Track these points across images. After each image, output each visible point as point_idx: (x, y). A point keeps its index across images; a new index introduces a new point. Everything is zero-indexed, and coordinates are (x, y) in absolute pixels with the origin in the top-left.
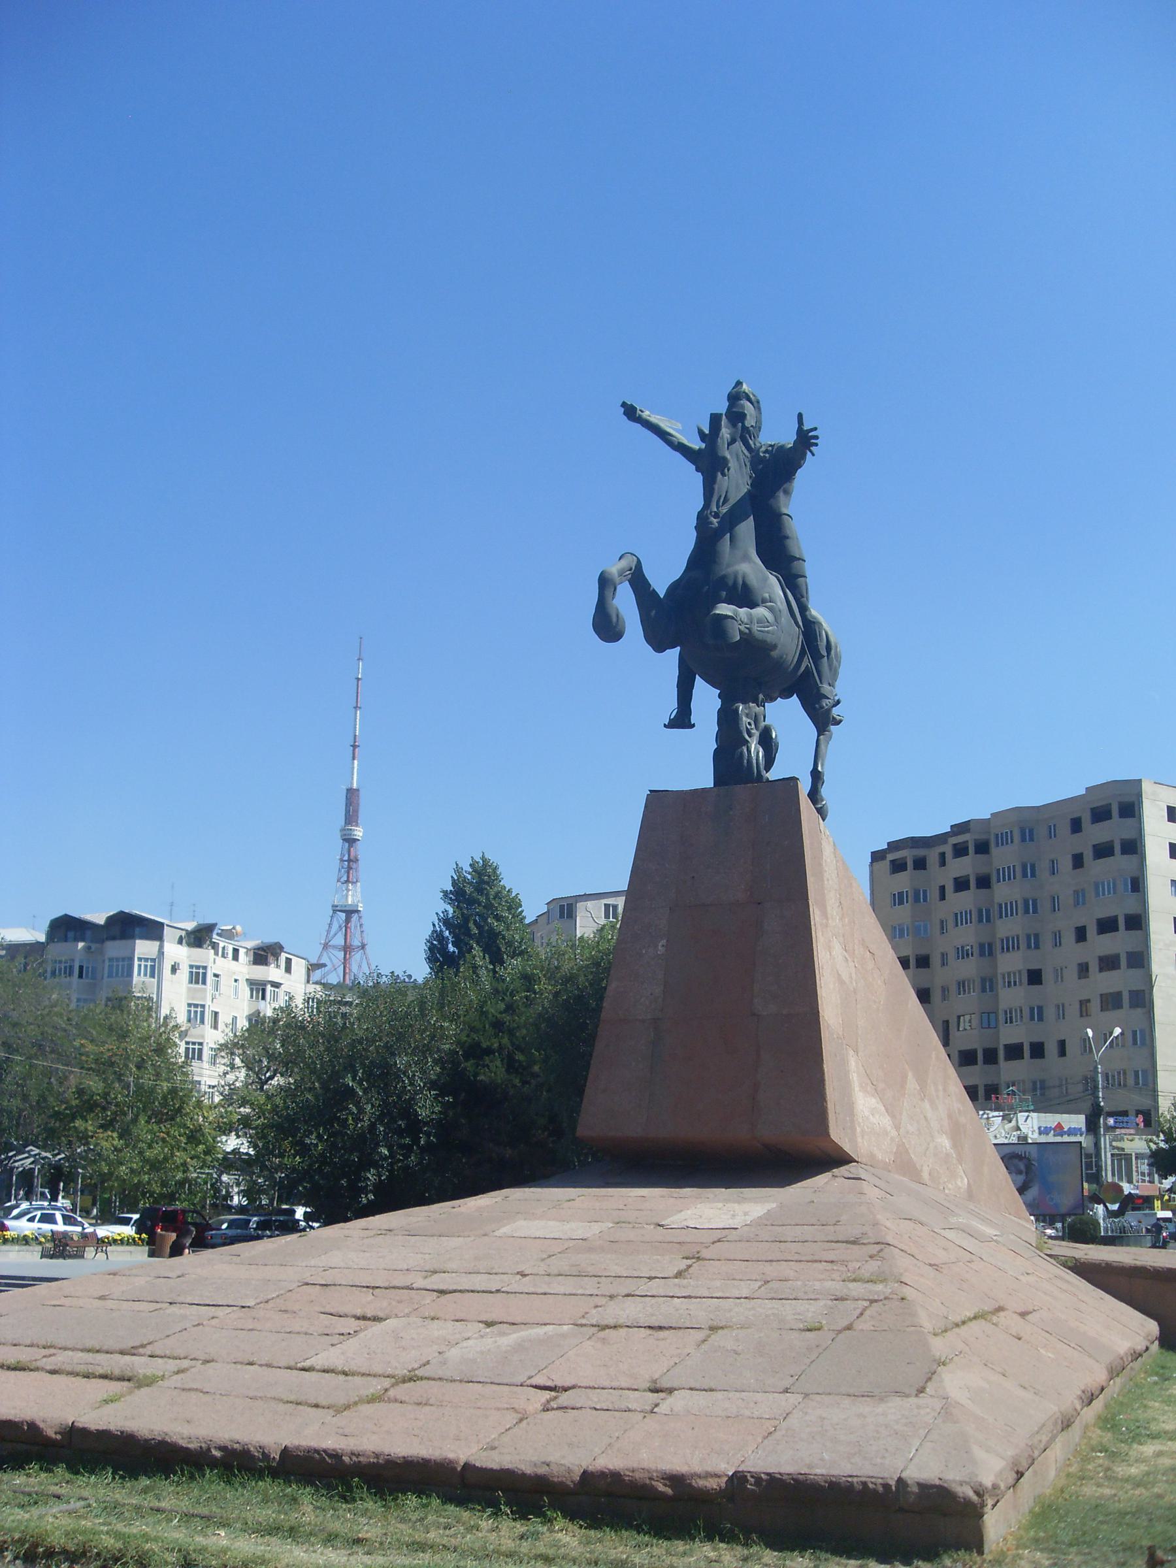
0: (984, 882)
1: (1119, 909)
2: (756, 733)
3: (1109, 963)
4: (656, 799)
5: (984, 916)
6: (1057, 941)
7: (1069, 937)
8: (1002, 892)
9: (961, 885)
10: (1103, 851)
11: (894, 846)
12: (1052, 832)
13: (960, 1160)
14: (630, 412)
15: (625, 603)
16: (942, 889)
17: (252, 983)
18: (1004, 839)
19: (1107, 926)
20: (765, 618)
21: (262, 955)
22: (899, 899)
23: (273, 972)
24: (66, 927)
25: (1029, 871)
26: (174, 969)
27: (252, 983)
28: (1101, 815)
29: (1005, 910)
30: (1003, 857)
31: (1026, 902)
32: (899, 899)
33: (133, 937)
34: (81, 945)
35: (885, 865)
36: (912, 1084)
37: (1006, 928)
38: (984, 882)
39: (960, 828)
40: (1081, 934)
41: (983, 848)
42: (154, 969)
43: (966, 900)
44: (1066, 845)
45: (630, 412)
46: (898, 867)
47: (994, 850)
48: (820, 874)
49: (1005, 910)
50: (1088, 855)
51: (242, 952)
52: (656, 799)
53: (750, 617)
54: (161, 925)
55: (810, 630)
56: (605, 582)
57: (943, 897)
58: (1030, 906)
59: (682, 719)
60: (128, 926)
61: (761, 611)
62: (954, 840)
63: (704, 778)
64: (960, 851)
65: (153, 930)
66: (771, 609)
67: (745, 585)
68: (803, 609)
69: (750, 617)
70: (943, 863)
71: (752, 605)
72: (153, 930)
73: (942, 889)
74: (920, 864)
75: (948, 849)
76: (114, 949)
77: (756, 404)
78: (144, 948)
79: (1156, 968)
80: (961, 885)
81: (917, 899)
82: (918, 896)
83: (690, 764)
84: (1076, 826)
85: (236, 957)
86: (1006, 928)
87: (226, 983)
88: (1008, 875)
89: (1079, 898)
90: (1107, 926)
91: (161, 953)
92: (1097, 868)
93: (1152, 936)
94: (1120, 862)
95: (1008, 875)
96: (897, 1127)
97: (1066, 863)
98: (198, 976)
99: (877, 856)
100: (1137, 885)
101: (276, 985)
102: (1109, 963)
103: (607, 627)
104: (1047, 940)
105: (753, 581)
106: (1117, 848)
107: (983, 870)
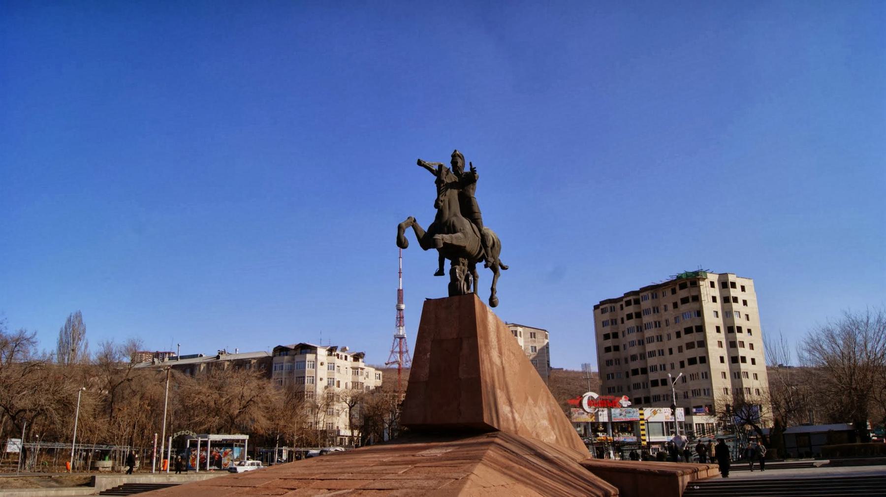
0: (638, 315)
1: (694, 323)
2: (463, 277)
3: (690, 346)
4: (428, 302)
5: (640, 329)
6: (669, 338)
7: (674, 336)
8: (646, 319)
9: (629, 317)
11: (602, 303)
13: (553, 428)
14: (420, 163)
15: (410, 235)
16: (622, 319)
17: (353, 368)
19: (688, 331)
20: (465, 237)
21: (357, 357)
22: (605, 324)
23: (360, 364)
24: (280, 350)
25: (656, 310)
26: (322, 364)
27: (353, 368)
29: (648, 326)
30: (646, 304)
31: (655, 323)
32: (605, 324)
33: (306, 353)
34: (286, 357)
35: (599, 311)
36: (530, 401)
37: (648, 333)
39: (627, 295)
40: (678, 335)
41: (637, 302)
42: (314, 366)
43: (632, 323)
45: (420, 163)
46: (603, 311)
47: (642, 303)
48: (485, 327)
49: (648, 326)
50: (679, 302)
51: (349, 357)
52: (428, 302)
53: (452, 238)
54: (315, 348)
55: (484, 238)
56: (400, 227)
57: (623, 322)
58: (657, 324)
59: (440, 273)
60: (305, 349)
61: (459, 234)
62: (625, 299)
63: (446, 294)
64: (628, 303)
65: (312, 349)
66: (463, 233)
67: (454, 226)
68: (480, 230)
69: (452, 238)
70: (622, 308)
71: (455, 232)
72: (312, 349)
73: (622, 319)
74: (613, 309)
75: (623, 303)
76: (298, 358)
77: (462, 157)
78: (310, 357)
79: (709, 347)
80: (629, 317)
81: (612, 324)
82: (614, 322)
83: (440, 289)
85: (346, 359)
86: (648, 333)
87: (342, 369)
88: (647, 312)
89: (676, 319)
90: (688, 331)
91: (316, 358)
92: (683, 308)
93: (708, 334)
94: (692, 306)
95: (647, 312)
96: (522, 418)
98: (331, 367)
99: (596, 307)
100: (700, 313)
101: (362, 369)
102: (690, 346)
103: (402, 243)
104: (665, 338)
105: (456, 223)
106: (690, 300)
107: (637, 311)
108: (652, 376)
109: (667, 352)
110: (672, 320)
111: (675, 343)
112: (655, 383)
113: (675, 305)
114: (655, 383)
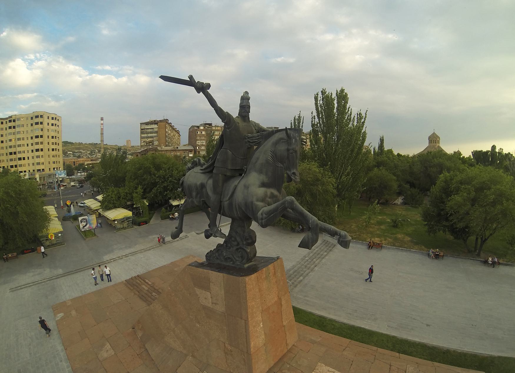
3: (37, 143)
7: (30, 138)
9: (10, 128)
10: (37, 123)
12: (27, 119)
18: (19, 119)
19: (37, 137)
28: (37, 117)
38: (14, 127)
39: (11, 117)
41: (14, 121)
44: (30, 122)
64: (10, 121)
80: (10, 128)
84: (32, 118)
90: (37, 137)
92: (36, 127)
97: (30, 125)
108: (19, 156)
109: (26, 145)
110: (29, 131)
111: (30, 141)
112: (20, 159)
113: (32, 125)
114: (20, 159)
